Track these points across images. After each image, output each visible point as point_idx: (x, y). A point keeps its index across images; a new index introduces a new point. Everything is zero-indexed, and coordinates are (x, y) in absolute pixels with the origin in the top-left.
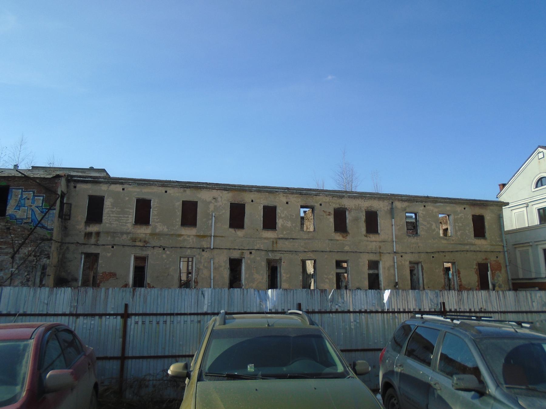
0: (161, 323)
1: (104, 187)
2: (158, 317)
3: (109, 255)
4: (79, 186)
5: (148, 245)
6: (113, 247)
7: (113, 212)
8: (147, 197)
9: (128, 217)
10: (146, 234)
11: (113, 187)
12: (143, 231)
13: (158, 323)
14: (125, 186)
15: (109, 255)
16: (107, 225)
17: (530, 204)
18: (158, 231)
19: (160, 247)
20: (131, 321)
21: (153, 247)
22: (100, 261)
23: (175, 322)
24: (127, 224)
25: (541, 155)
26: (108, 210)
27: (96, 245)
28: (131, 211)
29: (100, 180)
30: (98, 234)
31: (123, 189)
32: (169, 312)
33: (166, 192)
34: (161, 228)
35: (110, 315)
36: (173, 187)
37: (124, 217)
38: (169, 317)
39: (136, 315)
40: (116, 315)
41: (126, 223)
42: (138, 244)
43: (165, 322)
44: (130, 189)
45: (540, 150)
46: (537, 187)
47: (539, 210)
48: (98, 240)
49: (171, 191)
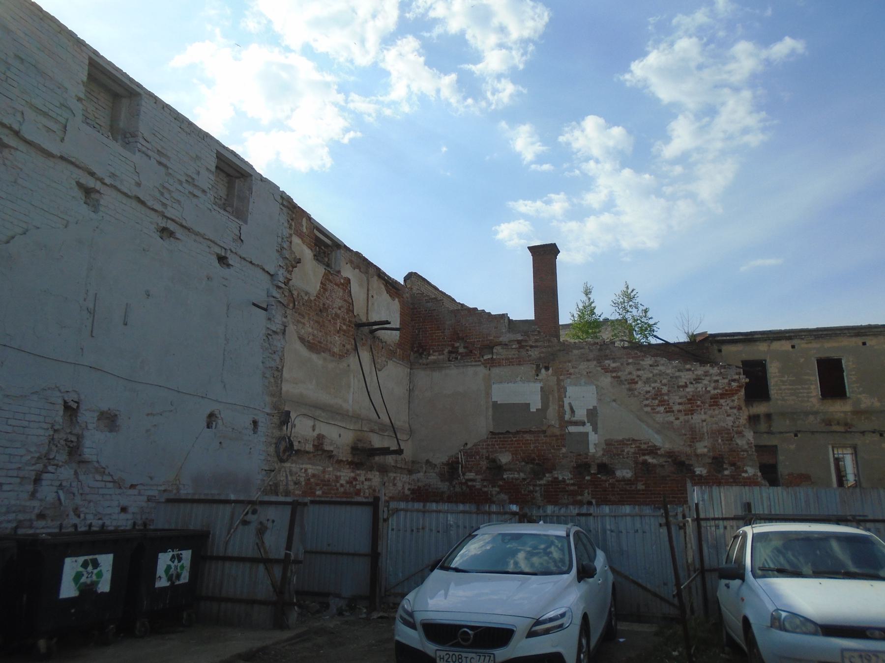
1: (763, 347)
3: (792, 447)
4: (727, 349)
5: (853, 429)
6: (796, 435)
7: (782, 381)
8: (834, 355)
9: (809, 388)
10: (845, 413)
11: (776, 346)
12: (838, 408)
14: (795, 342)
15: (792, 447)
16: (779, 402)
18: (863, 406)
19: (874, 432)
21: (863, 433)
22: (781, 458)
24: (812, 399)
26: (776, 379)
27: (770, 433)
28: (812, 378)
29: (756, 336)
30: (768, 416)
31: (793, 347)
33: (864, 344)
34: (867, 401)
36: (875, 335)
37: (803, 388)
41: (809, 397)
42: (835, 428)
44: (806, 346)
48: (770, 426)
49: (871, 342)
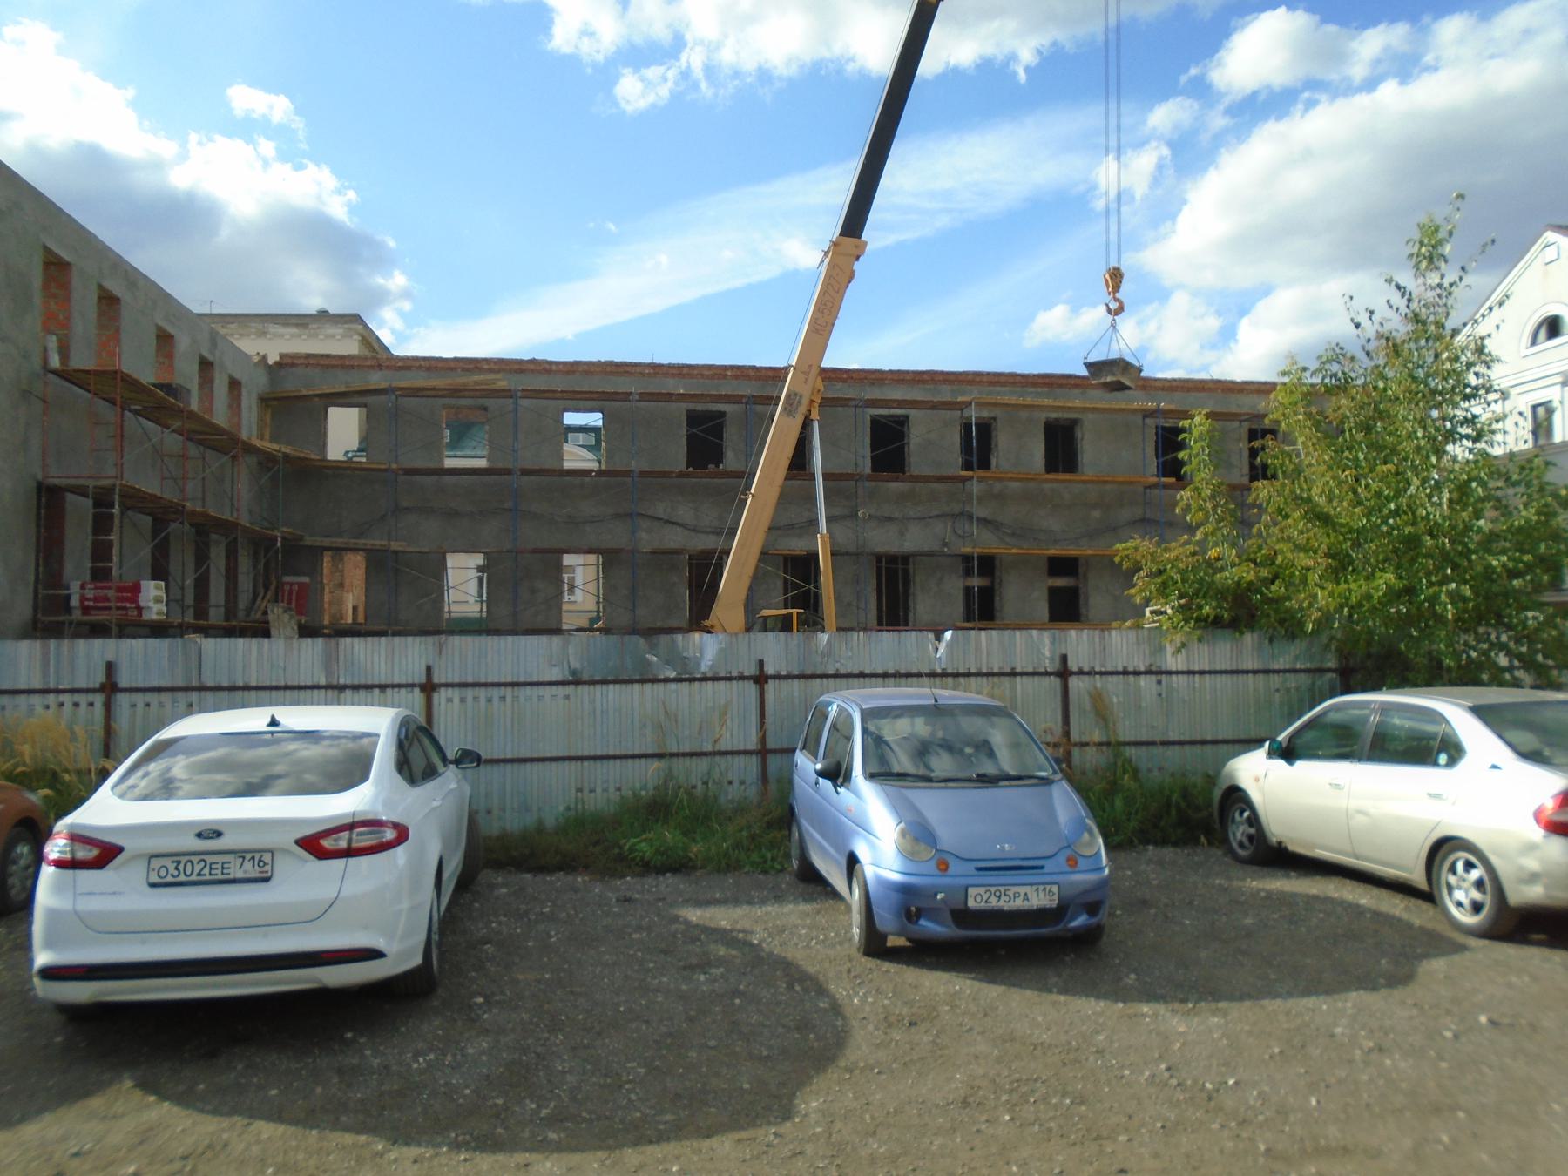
0: (496, 700)
2: (490, 689)
13: (490, 700)
17: (1513, 392)
20: (440, 697)
23: (522, 699)
25: (1550, 253)
32: (509, 680)
35: (399, 686)
38: (509, 690)
39: (447, 685)
40: (412, 686)
43: (503, 698)
45: (1550, 236)
46: (1534, 342)
47: (1534, 408)
